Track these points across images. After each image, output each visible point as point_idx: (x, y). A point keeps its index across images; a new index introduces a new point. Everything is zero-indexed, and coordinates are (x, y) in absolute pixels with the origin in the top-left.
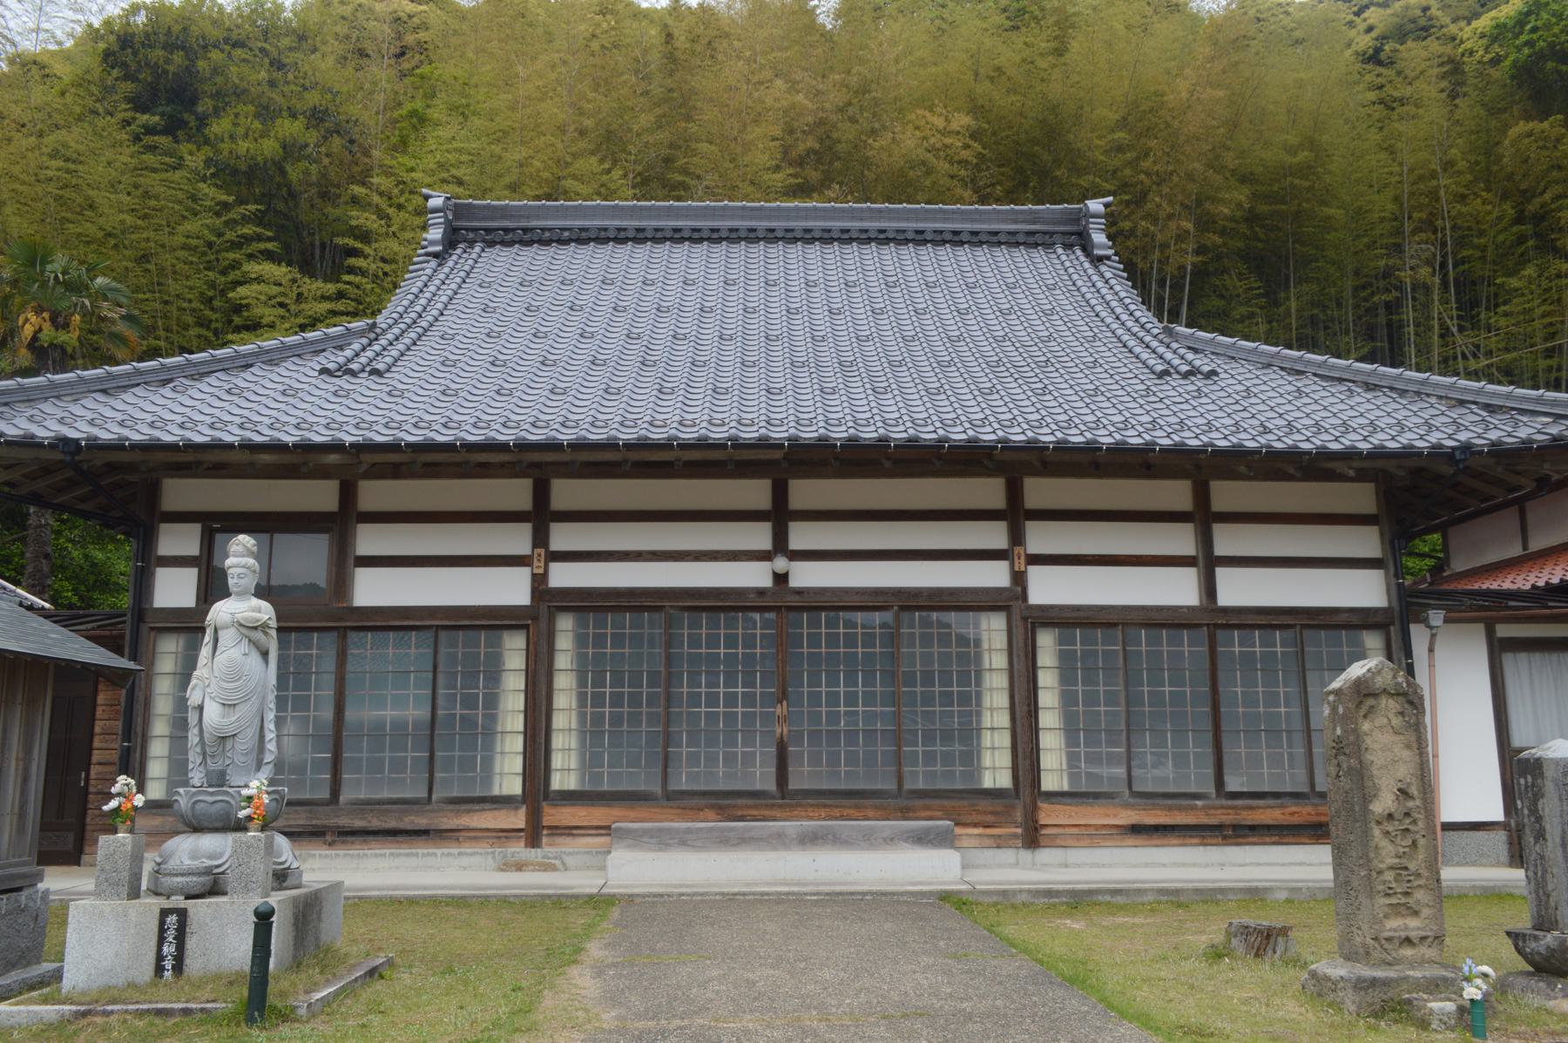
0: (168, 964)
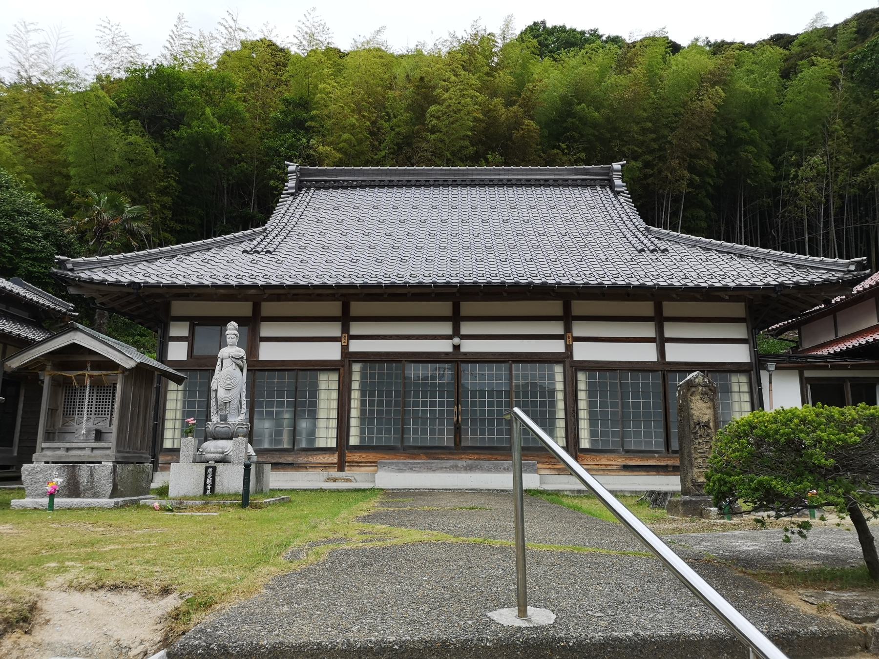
0: (209, 487)
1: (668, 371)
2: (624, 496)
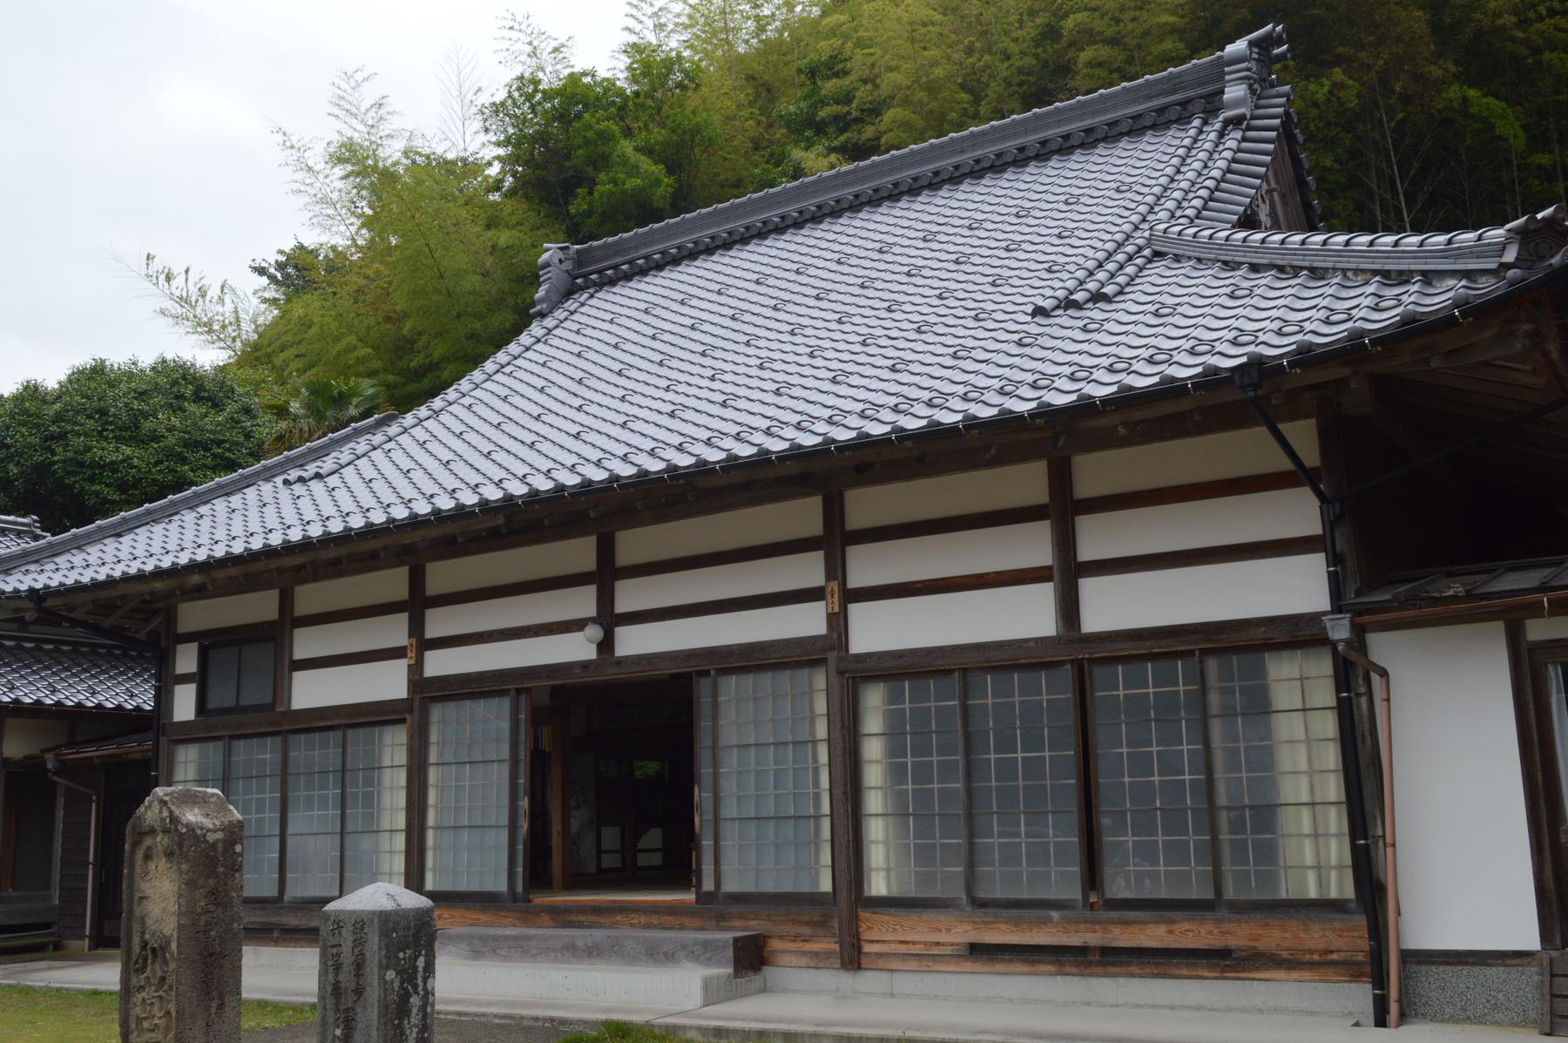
1: (1090, 660)
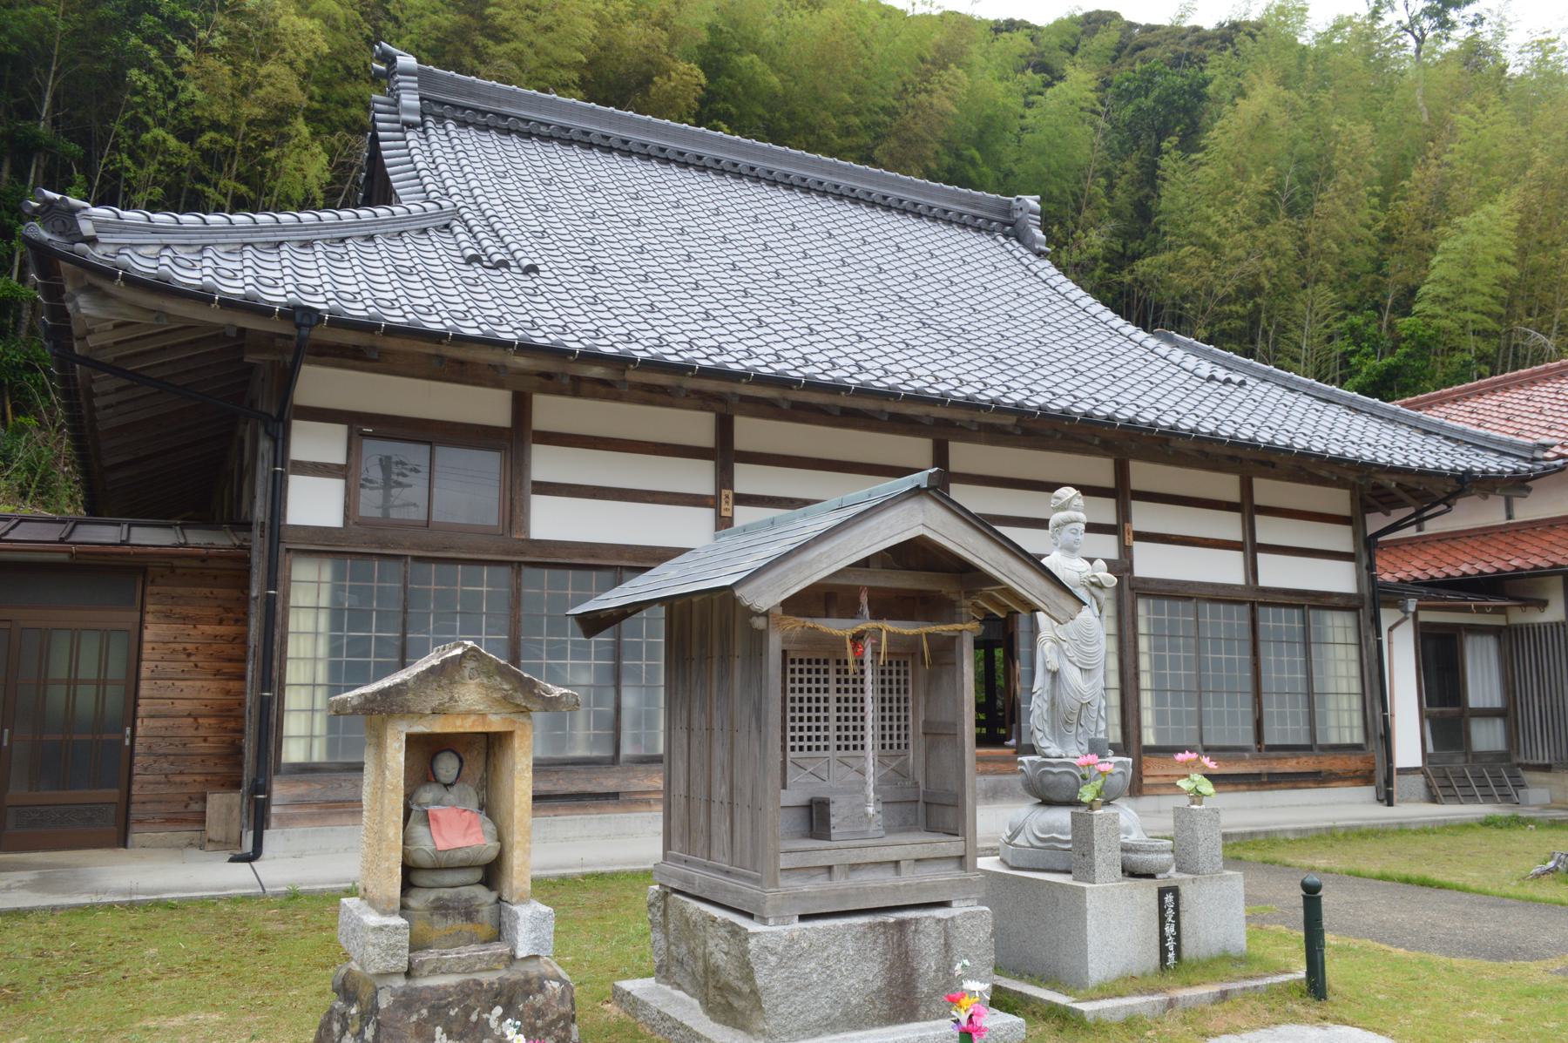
0: (1170, 945)
2: (1287, 840)
